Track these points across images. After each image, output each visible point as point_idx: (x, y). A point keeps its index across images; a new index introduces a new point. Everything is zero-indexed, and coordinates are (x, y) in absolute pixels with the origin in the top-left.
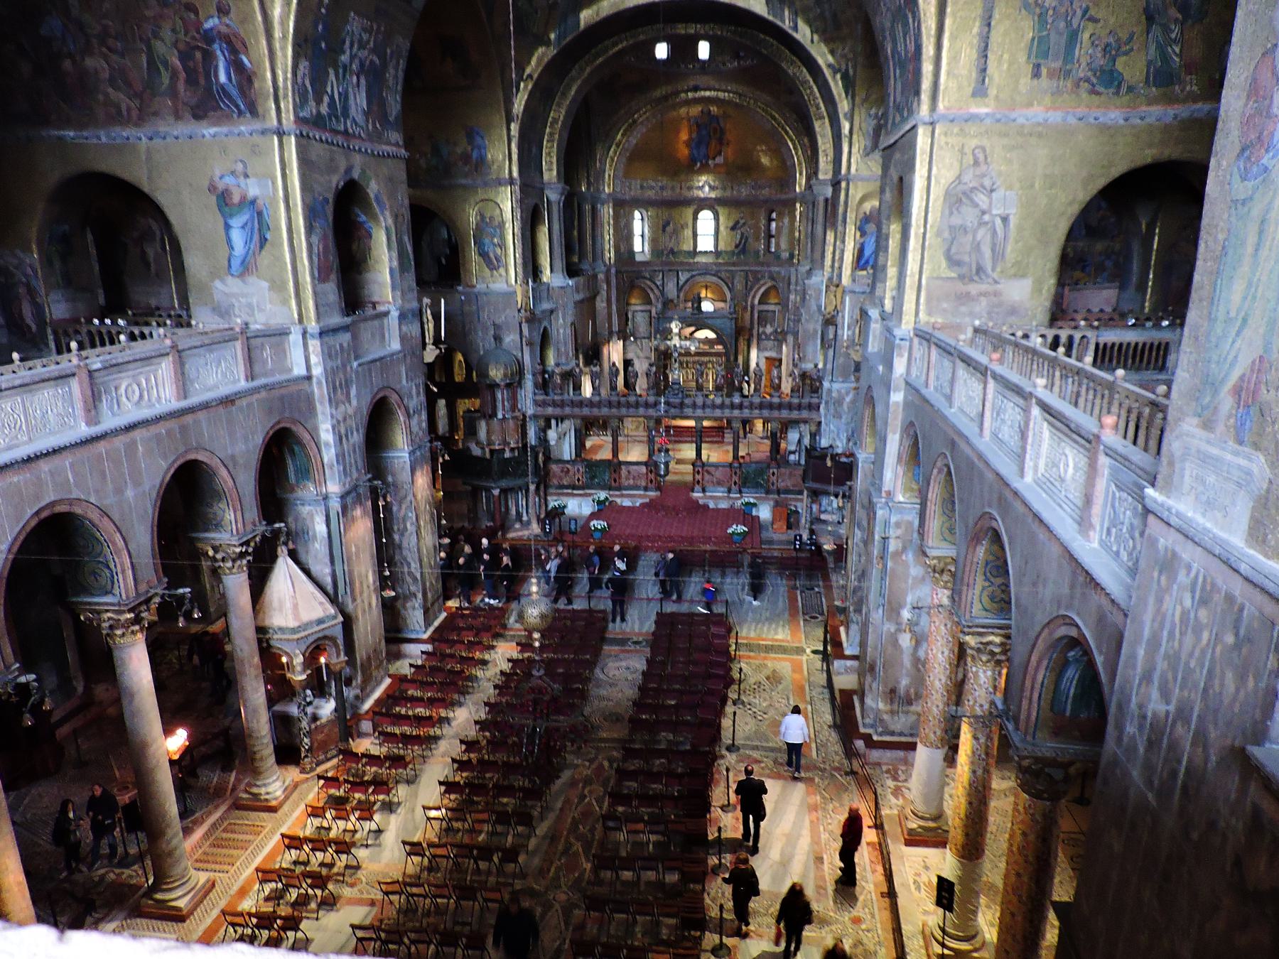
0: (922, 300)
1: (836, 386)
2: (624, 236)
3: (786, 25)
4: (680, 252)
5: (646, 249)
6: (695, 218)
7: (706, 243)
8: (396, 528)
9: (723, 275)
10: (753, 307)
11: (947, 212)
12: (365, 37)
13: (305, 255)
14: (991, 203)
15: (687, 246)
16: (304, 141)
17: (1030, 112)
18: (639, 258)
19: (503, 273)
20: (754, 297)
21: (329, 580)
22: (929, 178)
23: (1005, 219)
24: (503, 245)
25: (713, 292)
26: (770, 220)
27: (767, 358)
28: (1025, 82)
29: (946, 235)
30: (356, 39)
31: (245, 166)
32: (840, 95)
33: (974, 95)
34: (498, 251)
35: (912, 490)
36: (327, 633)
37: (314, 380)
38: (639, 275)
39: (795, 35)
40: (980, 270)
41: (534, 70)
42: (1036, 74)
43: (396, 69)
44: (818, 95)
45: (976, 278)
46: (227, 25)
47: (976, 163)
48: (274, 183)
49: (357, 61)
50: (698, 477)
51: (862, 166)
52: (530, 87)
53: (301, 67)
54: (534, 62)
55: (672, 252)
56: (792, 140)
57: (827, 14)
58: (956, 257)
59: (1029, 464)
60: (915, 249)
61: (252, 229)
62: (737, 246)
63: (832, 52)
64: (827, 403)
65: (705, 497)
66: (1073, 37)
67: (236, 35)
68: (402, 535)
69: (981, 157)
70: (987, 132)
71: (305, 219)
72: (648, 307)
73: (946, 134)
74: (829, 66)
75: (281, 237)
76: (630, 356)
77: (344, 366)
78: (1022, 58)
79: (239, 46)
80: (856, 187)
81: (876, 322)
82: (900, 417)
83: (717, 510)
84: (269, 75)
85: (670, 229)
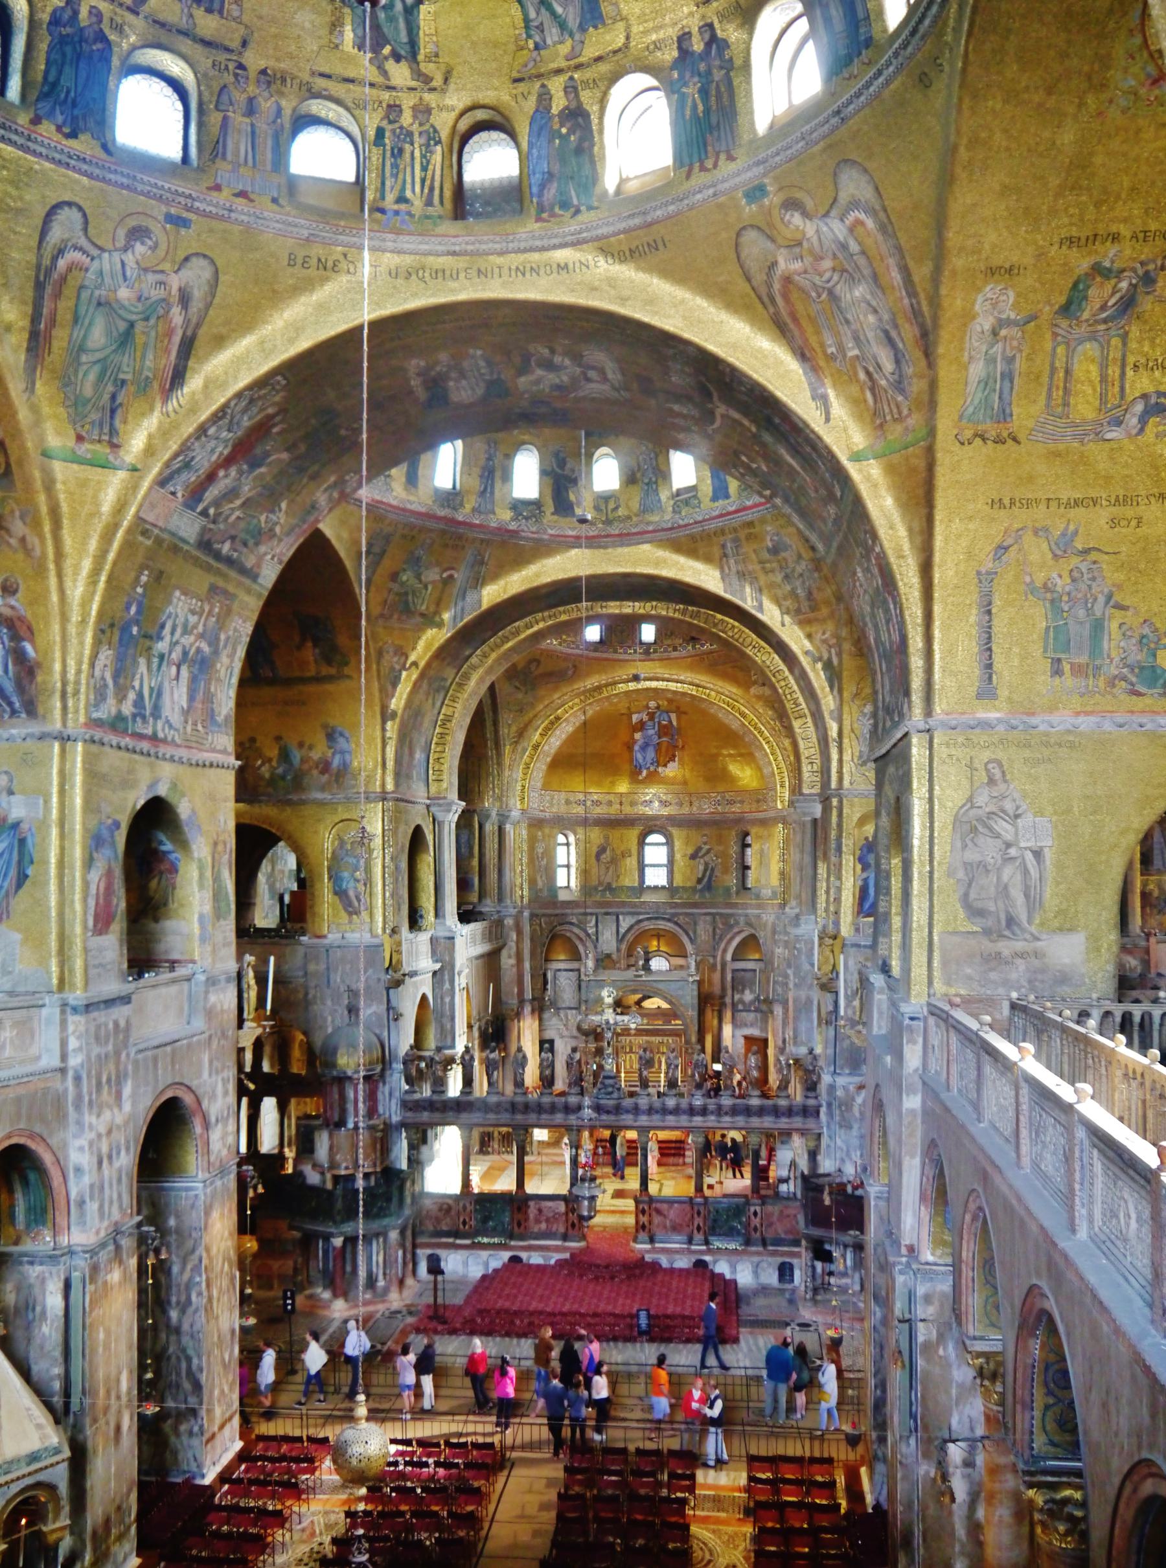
0: (936, 964)
1: (841, 1081)
2: (543, 865)
3: (749, 605)
4: (621, 888)
5: (573, 884)
6: (642, 843)
7: (656, 877)
8: (174, 1299)
9: (681, 920)
10: (724, 965)
11: (959, 844)
12: (193, 619)
13: (78, 897)
14: (1016, 834)
15: (630, 880)
16: (94, 748)
17: (1055, 718)
18: (563, 896)
20: (725, 951)
21: (57, 1385)
22: (931, 800)
23: (1038, 854)
24: (368, 882)
25: (668, 944)
26: (745, 846)
27: (746, 1038)
28: (1043, 680)
29: (961, 874)
30: (180, 621)
31: (11, 781)
32: (823, 689)
33: (979, 696)
34: (361, 888)
35: (944, 1243)
36: (41, 1477)
37: (71, 1074)
38: (562, 920)
39: (759, 615)
40: (1011, 921)
41: (420, 658)
42: (1057, 672)
43: (231, 656)
44: (795, 687)
45: (1007, 933)
46: (12, 607)
47: (991, 781)
48: (47, 802)
49: (179, 649)
50: (644, 1219)
51: (858, 778)
52: (414, 677)
53: (102, 656)
54: (421, 645)
55: (609, 887)
58: (979, 905)
59: (1081, 1211)
60: (920, 892)
61: (9, 863)
62: (699, 881)
63: (809, 636)
64: (829, 1105)
65: (654, 1250)
66: (1098, 627)
67: (21, 619)
68: (183, 1311)
69: (997, 773)
70: (1001, 741)
71: (84, 848)
72: (575, 965)
73: (948, 745)
74: (807, 653)
75: (47, 872)
76: (549, 1035)
77: (117, 1053)
78: (1037, 650)
79: (23, 632)
80: (852, 805)
82: (919, 1134)
83: (672, 1271)
84: (57, 667)
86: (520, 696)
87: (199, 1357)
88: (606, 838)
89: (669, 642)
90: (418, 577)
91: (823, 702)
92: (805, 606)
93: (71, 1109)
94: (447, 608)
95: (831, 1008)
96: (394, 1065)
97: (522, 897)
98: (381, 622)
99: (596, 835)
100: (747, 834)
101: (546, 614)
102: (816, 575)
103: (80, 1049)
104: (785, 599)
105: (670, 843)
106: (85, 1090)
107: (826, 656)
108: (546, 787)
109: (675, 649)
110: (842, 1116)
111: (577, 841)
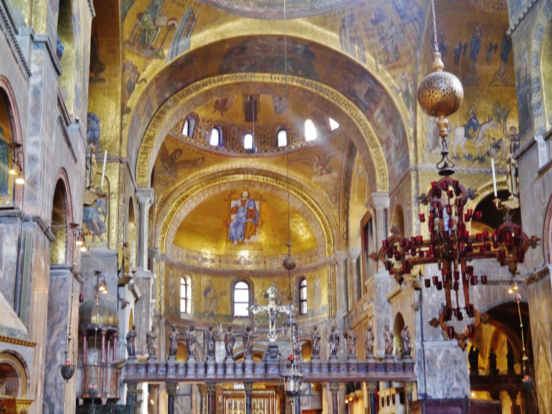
5: (189, 311)
6: (233, 289)
18: (183, 317)
19: (106, 239)
24: (107, 213)
26: (300, 287)
32: (403, 109)
34: (102, 218)
44: (372, 130)
54: (149, 68)
55: (212, 314)
56: (320, 216)
57: (390, 49)
63: (394, 77)
64: (420, 363)
74: (392, 87)
81: (542, 146)
85: (210, 294)
86: (167, 174)
87: (61, 403)
88: (210, 282)
89: (263, 147)
90: (154, 20)
91: (403, 116)
92: (392, 57)
93: (29, 115)
94: (168, 47)
95: (417, 299)
96: (121, 340)
97: (160, 310)
98: (127, 45)
99: (205, 280)
100: (303, 279)
101: (216, 78)
102: (402, 35)
103: (40, 72)
104: (379, 54)
105: (251, 289)
106: (42, 102)
107: (404, 88)
108: (175, 242)
109: (266, 151)
110: (430, 370)
111: (193, 282)
